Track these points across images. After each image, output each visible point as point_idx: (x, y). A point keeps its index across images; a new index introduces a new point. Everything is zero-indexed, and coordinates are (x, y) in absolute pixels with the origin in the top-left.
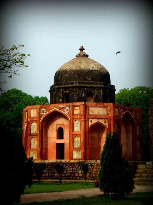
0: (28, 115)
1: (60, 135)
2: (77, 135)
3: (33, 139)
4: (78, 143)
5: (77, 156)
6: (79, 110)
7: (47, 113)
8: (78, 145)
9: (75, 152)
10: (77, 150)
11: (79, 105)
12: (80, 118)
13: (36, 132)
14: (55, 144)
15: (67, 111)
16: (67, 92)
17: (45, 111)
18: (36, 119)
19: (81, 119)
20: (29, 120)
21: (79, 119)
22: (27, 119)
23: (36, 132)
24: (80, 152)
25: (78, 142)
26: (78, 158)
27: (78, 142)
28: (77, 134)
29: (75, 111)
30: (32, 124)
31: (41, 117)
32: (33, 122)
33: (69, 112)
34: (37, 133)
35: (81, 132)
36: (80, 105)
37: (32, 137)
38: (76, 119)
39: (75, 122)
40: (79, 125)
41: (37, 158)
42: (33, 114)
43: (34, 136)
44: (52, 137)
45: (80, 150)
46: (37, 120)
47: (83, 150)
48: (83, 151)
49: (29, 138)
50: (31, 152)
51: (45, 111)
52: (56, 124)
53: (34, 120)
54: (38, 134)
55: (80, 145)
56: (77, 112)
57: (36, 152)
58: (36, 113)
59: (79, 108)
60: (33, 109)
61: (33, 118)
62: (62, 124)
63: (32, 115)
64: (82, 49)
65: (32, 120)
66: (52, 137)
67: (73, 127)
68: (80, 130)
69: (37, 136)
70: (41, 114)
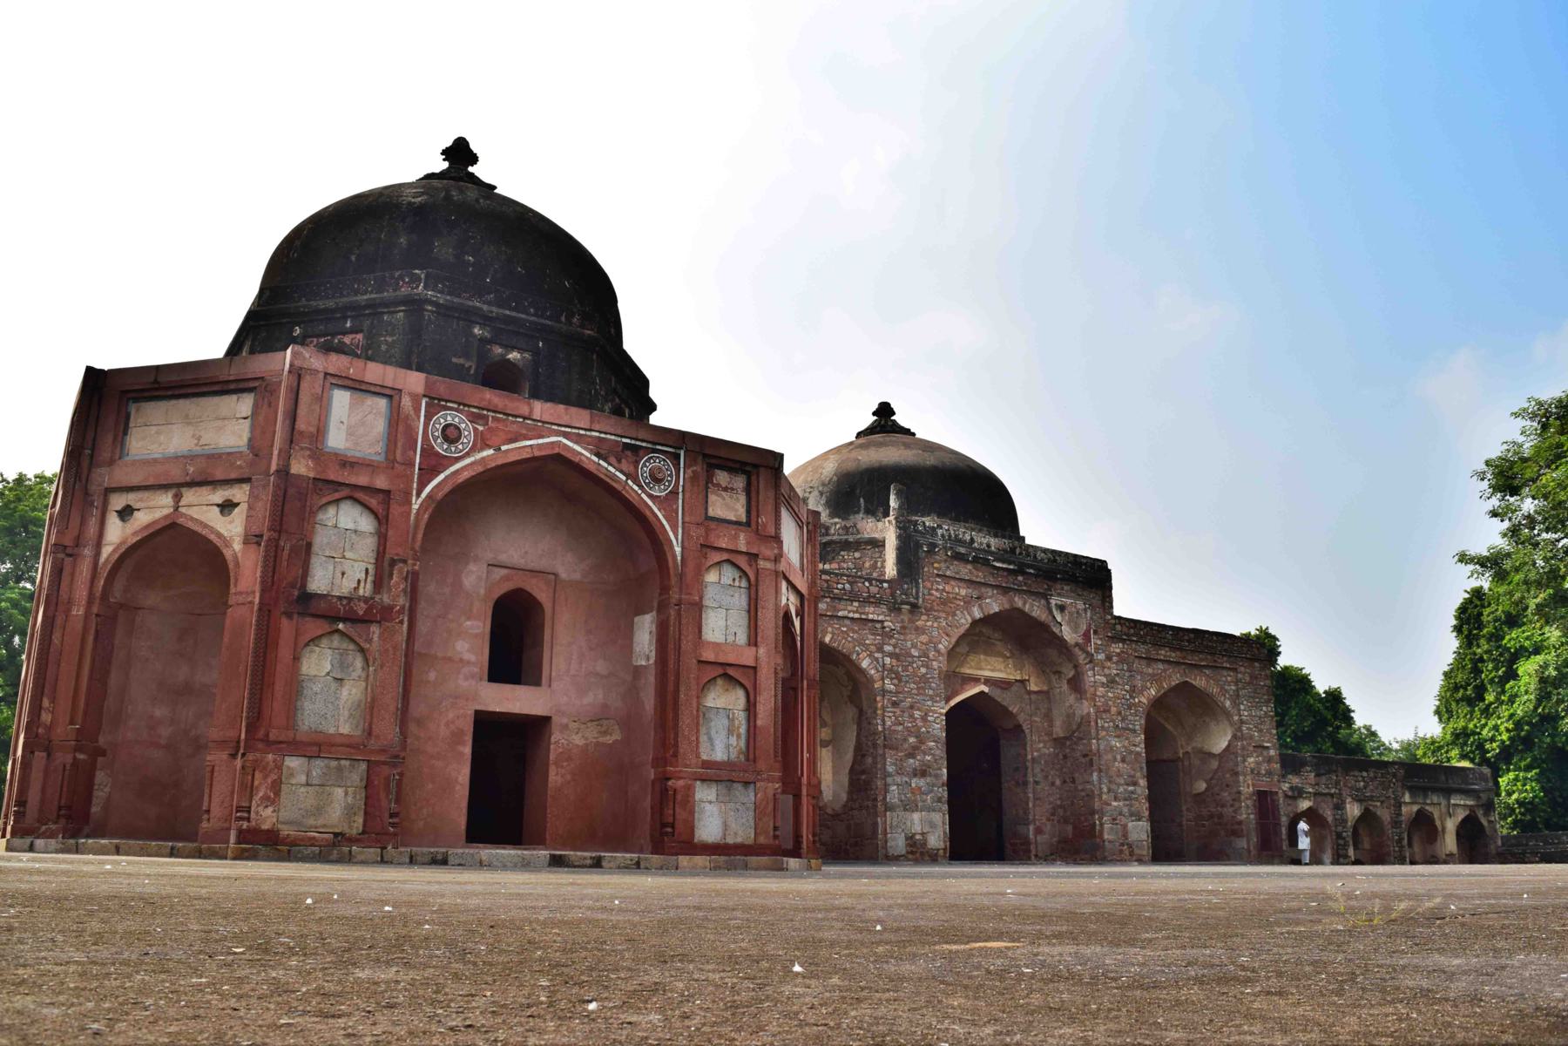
0: (301, 425)
1: (514, 642)
2: (728, 673)
3: (325, 642)
4: (730, 731)
5: (726, 826)
6: (743, 498)
7: (491, 452)
8: (733, 740)
9: (712, 797)
10: (717, 774)
11: (746, 464)
12: (753, 557)
13: (366, 590)
14: (471, 713)
15: (656, 479)
16: (514, 356)
17: (468, 437)
18: (381, 482)
19: (762, 564)
20: (301, 467)
21: (742, 562)
22: (286, 456)
23: (366, 590)
24: (748, 797)
25: (731, 720)
26: (730, 840)
27: (731, 720)
28: (731, 659)
29: (712, 498)
30: (331, 511)
31: (428, 472)
32: (354, 495)
33: (674, 493)
34: (386, 599)
35: (762, 651)
36: (756, 466)
37: (325, 626)
38: (725, 556)
39: (711, 577)
40: (740, 600)
41: (361, 820)
42: (350, 433)
43: (344, 620)
44: (444, 658)
45: (746, 784)
46: (387, 493)
47: (768, 780)
48: (770, 793)
49: (286, 627)
50: (292, 763)
51: (468, 437)
52: (489, 556)
53: (362, 480)
54: (391, 608)
55: (743, 743)
56: (728, 507)
57: (357, 775)
58: (380, 426)
59: (739, 482)
60: (358, 387)
61: (346, 463)
62: (531, 566)
63: (336, 439)
64: (460, 153)
65: (332, 477)
66: (440, 655)
67: (698, 607)
68: (742, 638)
69: (375, 630)
70: (428, 451)
